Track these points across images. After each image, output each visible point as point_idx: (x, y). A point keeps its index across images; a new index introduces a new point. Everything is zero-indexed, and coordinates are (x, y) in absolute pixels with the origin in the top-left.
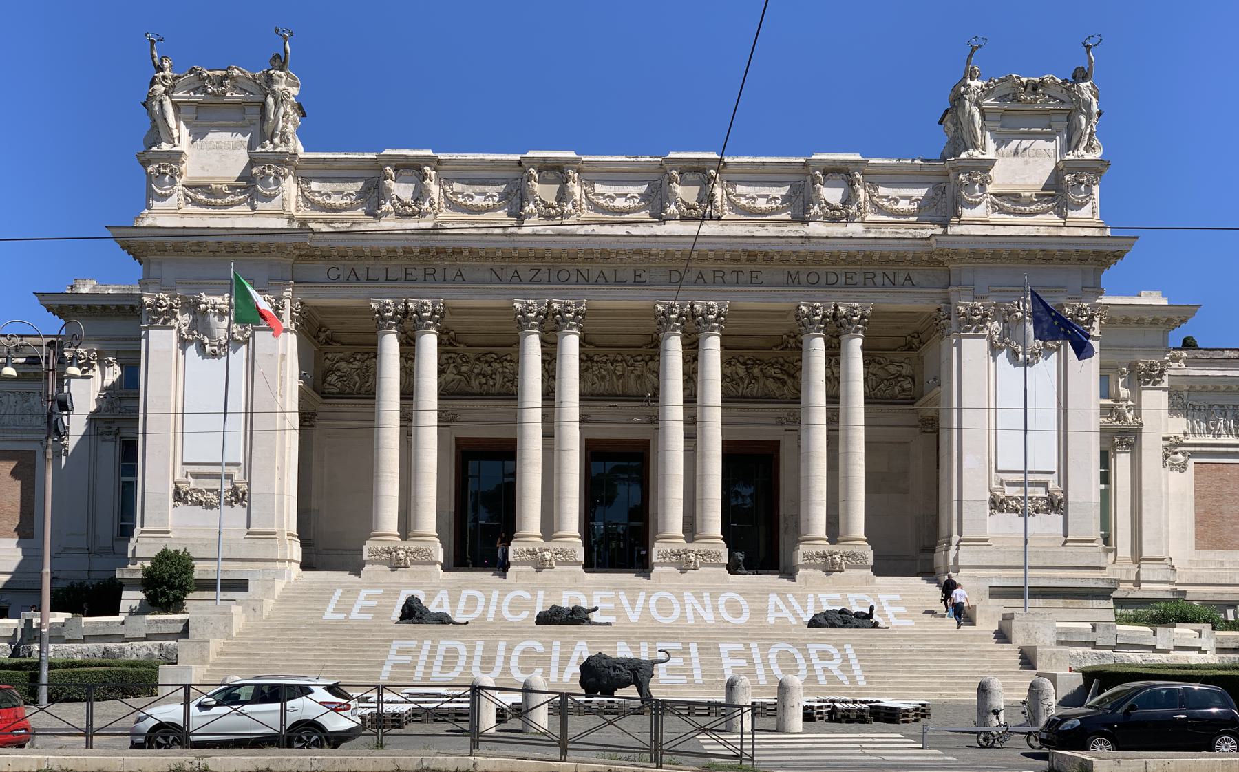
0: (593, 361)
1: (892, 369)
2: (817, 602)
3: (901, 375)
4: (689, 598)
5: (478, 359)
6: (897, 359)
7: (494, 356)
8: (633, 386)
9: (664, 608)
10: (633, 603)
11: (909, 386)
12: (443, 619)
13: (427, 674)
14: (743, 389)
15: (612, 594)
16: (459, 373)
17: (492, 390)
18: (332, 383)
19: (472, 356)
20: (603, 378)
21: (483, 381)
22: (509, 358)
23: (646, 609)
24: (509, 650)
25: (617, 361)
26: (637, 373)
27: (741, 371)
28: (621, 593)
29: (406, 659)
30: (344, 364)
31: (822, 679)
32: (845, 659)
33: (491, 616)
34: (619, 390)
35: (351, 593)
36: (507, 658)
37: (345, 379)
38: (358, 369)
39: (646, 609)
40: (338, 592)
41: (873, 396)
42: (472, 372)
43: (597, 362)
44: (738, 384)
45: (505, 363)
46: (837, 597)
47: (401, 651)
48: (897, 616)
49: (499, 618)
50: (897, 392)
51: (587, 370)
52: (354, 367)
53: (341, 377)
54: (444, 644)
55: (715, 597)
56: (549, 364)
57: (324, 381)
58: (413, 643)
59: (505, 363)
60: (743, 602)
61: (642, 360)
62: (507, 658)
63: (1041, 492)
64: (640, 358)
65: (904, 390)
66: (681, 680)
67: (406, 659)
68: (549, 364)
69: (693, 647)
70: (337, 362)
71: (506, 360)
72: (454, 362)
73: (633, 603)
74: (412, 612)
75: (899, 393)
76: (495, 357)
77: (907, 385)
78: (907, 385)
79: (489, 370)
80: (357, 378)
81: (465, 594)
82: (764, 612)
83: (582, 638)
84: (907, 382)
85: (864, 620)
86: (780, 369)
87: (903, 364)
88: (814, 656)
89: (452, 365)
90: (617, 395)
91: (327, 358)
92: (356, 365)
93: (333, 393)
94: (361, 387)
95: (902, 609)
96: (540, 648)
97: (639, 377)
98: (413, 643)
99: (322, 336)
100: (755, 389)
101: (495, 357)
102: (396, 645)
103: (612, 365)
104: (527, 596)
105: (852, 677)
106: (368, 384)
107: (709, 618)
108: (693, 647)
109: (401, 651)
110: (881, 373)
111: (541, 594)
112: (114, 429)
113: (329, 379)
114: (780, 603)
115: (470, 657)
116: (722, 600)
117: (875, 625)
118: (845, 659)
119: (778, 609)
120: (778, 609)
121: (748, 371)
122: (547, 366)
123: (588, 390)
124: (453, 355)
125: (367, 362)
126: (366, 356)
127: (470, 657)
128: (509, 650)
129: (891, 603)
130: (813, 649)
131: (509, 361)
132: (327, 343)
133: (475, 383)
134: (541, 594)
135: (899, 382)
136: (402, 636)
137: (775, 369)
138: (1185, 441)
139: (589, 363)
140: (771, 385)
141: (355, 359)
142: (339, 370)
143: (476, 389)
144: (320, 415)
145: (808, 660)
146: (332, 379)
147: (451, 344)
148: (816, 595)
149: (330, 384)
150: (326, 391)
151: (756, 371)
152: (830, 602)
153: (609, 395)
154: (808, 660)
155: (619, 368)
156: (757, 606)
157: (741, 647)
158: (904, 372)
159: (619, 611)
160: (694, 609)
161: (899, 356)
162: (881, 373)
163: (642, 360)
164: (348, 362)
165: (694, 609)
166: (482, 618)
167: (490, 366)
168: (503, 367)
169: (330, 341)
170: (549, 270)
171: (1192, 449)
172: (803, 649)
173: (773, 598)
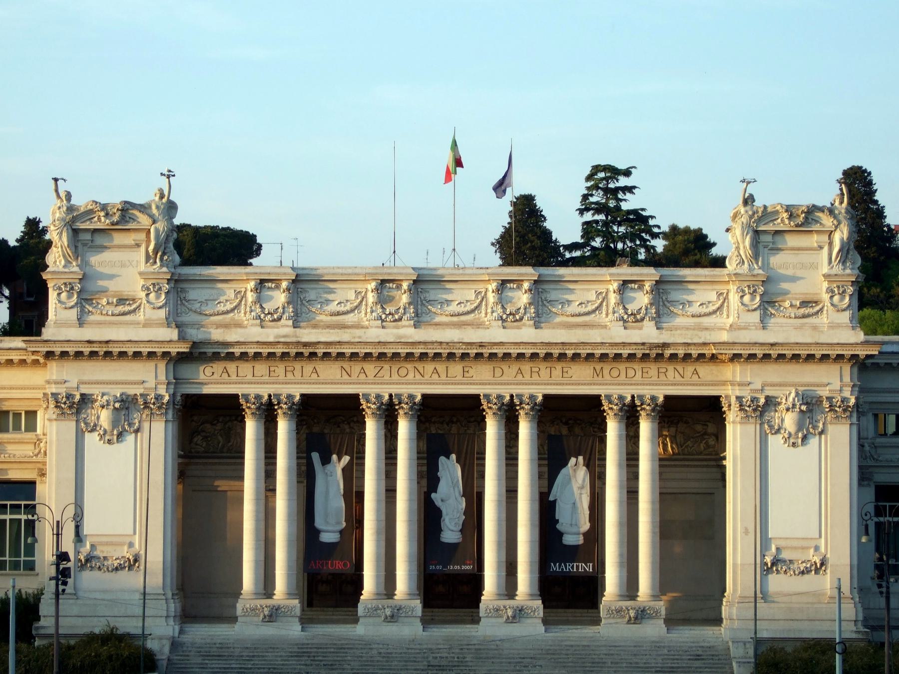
1: (699, 428)
3: (706, 433)
7: (341, 417)
11: (713, 443)
18: (199, 442)
22: (355, 419)
25: (453, 422)
27: (565, 431)
30: (208, 426)
37: (209, 439)
38: (220, 430)
41: (681, 453)
43: (434, 423)
45: (352, 424)
50: (702, 448)
52: (217, 428)
53: (206, 437)
56: (391, 425)
57: (191, 442)
59: (352, 424)
61: (475, 421)
64: (472, 419)
65: (708, 446)
68: (391, 425)
70: (201, 425)
71: (353, 421)
72: (306, 424)
75: (705, 449)
76: (344, 419)
77: (712, 441)
80: (220, 438)
84: (712, 439)
86: (599, 428)
87: (707, 423)
89: (305, 427)
91: (193, 421)
92: (219, 426)
93: (198, 452)
94: (223, 446)
101: (344, 419)
103: (448, 425)
106: (230, 444)
113: (195, 439)
121: (570, 429)
122: (389, 427)
124: (305, 418)
125: (230, 424)
126: (228, 418)
131: (355, 422)
135: (705, 439)
137: (594, 428)
139: (427, 424)
141: (218, 421)
142: (204, 431)
146: (198, 439)
149: (197, 444)
150: (193, 450)
163: (475, 421)
164: (213, 425)
167: (339, 427)
168: (350, 428)
170: (391, 367)
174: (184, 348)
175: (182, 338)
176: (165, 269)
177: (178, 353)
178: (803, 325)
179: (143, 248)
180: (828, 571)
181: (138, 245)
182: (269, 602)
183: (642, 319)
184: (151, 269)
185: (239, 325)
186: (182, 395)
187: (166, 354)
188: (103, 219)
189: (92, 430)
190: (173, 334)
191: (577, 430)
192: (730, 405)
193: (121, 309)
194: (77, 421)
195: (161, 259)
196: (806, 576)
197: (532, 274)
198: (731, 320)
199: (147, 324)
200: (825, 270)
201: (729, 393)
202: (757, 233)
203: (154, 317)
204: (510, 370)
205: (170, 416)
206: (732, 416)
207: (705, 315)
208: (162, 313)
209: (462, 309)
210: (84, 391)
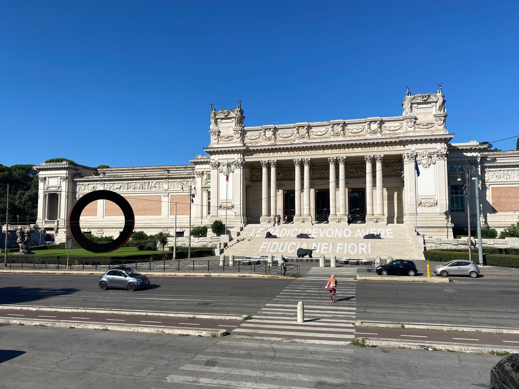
0: (316, 170)
1: (395, 168)
2: (369, 231)
4: (337, 230)
5: (288, 171)
6: (396, 165)
8: (326, 176)
9: (330, 233)
10: (322, 231)
12: (275, 237)
13: (268, 252)
14: (355, 175)
15: (317, 229)
16: (284, 174)
17: (292, 178)
19: (287, 170)
20: (319, 174)
21: (289, 176)
23: (325, 233)
24: (288, 245)
26: (327, 172)
27: (354, 170)
28: (320, 229)
29: (265, 247)
31: (360, 253)
32: (368, 247)
33: (288, 235)
34: (323, 177)
35: (257, 229)
36: (287, 247)
39: (325, 233)
40: (254, 229)
42: (286, 174)
44: (353, 174)
46: (375, 230)
47: (265, 245)
48: (389, 235)
49: (290, 236)
51: (315, 172)
54: (274, 243)
55: (343, 230)
57: (252, 178)
58: (267, 243)
60: (350, 232)
62: (287, 247)
63: (432, 201)
66: (326, 252)
67: (265, 247)
69: (331, 244)
73: (322, 231)
74: (269, 235)
78: (399, 172)
79: (291, 173)
81: (283, 229)
82: (355, 234)
83: (305, 242)
85: (378, 237)
88: (360, 246)
90: (322, 178)
92: (259, 173)
95: (391, 233)
96: (295, 244)
97: (328, 173)
98: (267, 243)
99: (252, 167)
100: (358, 174)
102: (264, 243)
104: (297, 230)
105: (368, 252)
107: (340, 236)
108: (331, 244)
109: (265, 245)
110: (392, 169)
111: (300, 229)
112: (207, 190)
114: (360, 231)
115: (279, 247)
116: (345, 231)
117: (380, 238)
118: (368, 247)
119: (358, 233)
120: (358, 233)
123: (314, 176)
127: (279, 247)
128: (288, 245)
129: (389, 231)
130: (360, 245)
132: (253, 169)
133: (287, 177)
134: (300, 229)
136: (265, 242)
138: (489, 181)
140: (362, 173)
143: (288, 178)
144: (251, 186)
145: (358, 247)
146: (254, 177)
147: (281, 167)
148: (370, 229)
151: (358, 170)
152: (373, 231)
153: (320, 178)
154: (358, 247)
155: (323, 171)
156: (353, 232)
157: (342, 244)
158: (398, 168)
159: (318, 234)
160: (337, 233)
161: (397, 164)
162: (392, 169)
165: (337, 233)
166: (285, 236)
169: (253, 168)
171: (490, 183)
172: (358, 245)
173: (358, 230)
174: (245, 148)
175: (244, 145)
176: (240, 127)
177: (243, 150)
178: (427, 131)
179: (234, 123)
180: (439, 205)
181: (233, 122)
182: (268, 218)
183: (376, 133)
184: (236, 127)
185: (260, 142)
186: (245, 162)
187: (240, 150)
188: (223, 115)
189: (221, 172)
190: (241, 145)
191: (358, 170)
192: (405, 157)
193: (228, 139)
194: (218, 170)
195: (239, 125)
196: (431, 207)
197: (343, 122)
198: (404, 131)
199: (236, 142)
200: (435, 113)
201: (405, 153)
202: (412, 104)
203: (237, 141)
204: (336, 151)
205: (242, 167)
206: (406, 160)
207: (396, 130)
208: (239, 139)
209: (322, 133)
210: (219, 162)
